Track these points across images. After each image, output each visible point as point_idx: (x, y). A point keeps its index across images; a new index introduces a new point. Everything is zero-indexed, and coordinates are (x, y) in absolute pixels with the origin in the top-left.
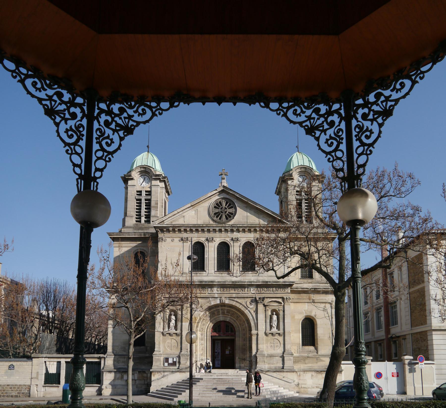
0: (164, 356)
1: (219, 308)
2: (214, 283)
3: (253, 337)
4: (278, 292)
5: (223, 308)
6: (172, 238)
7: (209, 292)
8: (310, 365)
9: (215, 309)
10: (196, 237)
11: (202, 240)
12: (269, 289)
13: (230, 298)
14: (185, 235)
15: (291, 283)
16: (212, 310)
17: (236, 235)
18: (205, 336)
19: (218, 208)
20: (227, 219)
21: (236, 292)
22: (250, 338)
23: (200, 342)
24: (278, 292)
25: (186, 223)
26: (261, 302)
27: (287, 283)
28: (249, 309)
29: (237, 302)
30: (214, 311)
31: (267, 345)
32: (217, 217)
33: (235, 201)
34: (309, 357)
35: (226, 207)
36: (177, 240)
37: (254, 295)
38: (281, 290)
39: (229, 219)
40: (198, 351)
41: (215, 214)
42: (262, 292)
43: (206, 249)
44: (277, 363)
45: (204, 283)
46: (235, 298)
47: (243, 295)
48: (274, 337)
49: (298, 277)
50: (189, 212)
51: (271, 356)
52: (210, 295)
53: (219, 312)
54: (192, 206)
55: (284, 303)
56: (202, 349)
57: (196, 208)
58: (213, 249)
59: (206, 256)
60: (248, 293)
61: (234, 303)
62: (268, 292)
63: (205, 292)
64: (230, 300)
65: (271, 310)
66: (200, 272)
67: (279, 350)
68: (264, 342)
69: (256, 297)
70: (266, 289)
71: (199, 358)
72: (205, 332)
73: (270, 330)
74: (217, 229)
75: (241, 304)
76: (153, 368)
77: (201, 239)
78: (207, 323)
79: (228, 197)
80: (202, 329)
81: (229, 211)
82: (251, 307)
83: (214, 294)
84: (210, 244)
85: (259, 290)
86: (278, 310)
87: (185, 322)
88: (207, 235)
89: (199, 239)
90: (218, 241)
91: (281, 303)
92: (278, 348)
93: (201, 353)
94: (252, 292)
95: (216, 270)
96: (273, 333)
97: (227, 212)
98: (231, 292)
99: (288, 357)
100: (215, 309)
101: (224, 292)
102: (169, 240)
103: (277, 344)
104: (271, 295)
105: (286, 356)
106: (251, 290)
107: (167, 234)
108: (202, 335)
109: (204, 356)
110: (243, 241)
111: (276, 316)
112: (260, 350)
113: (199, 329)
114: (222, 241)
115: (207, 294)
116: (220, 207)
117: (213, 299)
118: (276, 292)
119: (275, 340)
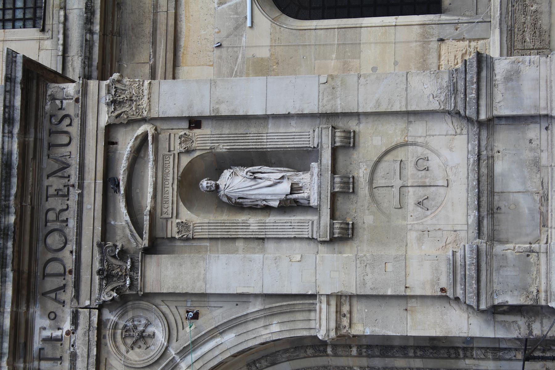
3: (358, 329)
4: (74, 161)
12: (51, 216)
15: (19, 75)
22: (369, 347)
24: (74, 161)
26: (133, 267)
27: (18, 102)
28: (172, 352)
31: (412, 236)
37: (83, 315)
38: (64, 139)
42: (70, 264)
44: (536, 164)
49: (35, 44)
55: (144, 120)
60: (74, 357)
62: (72, 223)
65: (183, 209)
67: (445, 153)
68: (392, 252)
69: (100, 308)
70: (54, 240)
73: (316, 210)
82: (161, 337)
85: (57, 282)
86: (185, 160)
91: (143, 139)
92: (434, 162)
94: (67, 326)
96: (334, 195)
99: (498, 97)
103: (410, 170)
104: (88, 205)
105: (490, 106)
106: (58, 333)
111: (227, 173)
112: (444, 282)
118: (74, 172)
119: (379, 181)
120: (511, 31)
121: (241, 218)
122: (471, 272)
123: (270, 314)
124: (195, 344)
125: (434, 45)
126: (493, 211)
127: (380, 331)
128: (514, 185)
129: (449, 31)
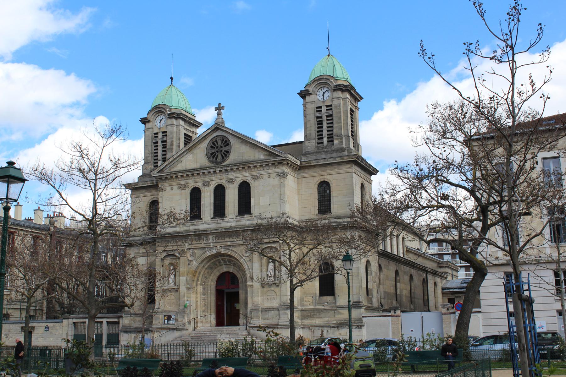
0: (164, 313)
1: (218, 258)
2: (208, 232)
3: (249, 289)
5: (223, 258)
6: (171, 187)
7: (205, 242)
8: (326, 319)
9: (215, 260)
10: (192, 183)
11: (199, 185)
13: (226, 247)
14: (183, 182)
16: (212, 261)
17: (231, 175)
18: (208, 289)
19: (214, 148)
20: (223, 157)
21: (231, 239)
23: (201, 297)
25: (184, 168)
28: (244, 258)
29: (232, 250)
30: (215, 261)
32: (213, 157)
33: (230, 138)
34: (326, 310)
35: (222, 145)
36: (175, 188)
39: (225, 158)
40: (199, 307)
41: (212, 154)
43: (202, 194)
44: (273, 318)
45: (198, 233)
46: (230, 246)
47: (237, 242)
48: (270, 289)
50: (186, 156)
51: (266, 310)
52: (205, 245)
53: (220, 262)
54: (187, 150)
56: (205, 305)
57: (192, 151)
58: (208, 194)
59: (202, 203)
61: (229, 252)
63: (200, 242)
64: (225, 249)
66: (197, 221)
71: (201, 315)
72: (208, 285)
74: (212, 171)
75: (236, 253)
76: (153, 327)
77: (198, 184)
78: (210, 275)
79: (223, 134)
80: (204, 282)
81: (224, 149)
82: (247, 255)
83: (210, 243)
84: (207, 188)
87: (182, 276)
88: (203, 179)
89: (196, 184)
90: (214, 184)
92: (274, 301)
93: (204, 309)
95: (212, 216)
97: (223, 151)
98: (225, 240)
100: (215, 260)
101: (219, 241)
102: (168, 188)
103: (273, 297)
107: (167, 183)
108: (204, 289)
109: (208, 312)
110: (239, 181)
113: (199, 283)
114: (218, 184)
115: (203, 245)
116: (215, 146)
117: (209, 249)
120: (314, 310)
121: (265, 268)
122: (256, 308)
123: (250, 274)
124: (245, 261)
125: (312, 296)
126: (266, 311)
127: (248, 293)
128: (270, 314)
129: (314, 298)
